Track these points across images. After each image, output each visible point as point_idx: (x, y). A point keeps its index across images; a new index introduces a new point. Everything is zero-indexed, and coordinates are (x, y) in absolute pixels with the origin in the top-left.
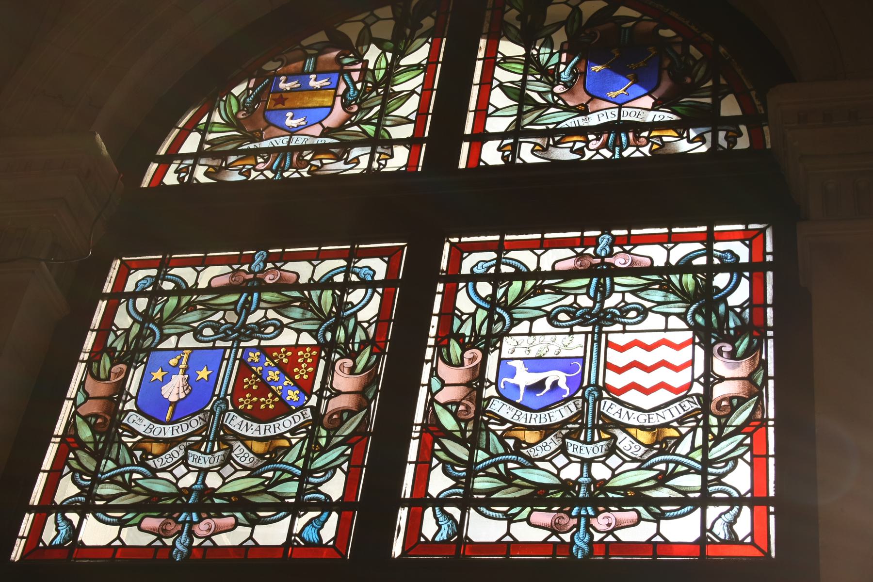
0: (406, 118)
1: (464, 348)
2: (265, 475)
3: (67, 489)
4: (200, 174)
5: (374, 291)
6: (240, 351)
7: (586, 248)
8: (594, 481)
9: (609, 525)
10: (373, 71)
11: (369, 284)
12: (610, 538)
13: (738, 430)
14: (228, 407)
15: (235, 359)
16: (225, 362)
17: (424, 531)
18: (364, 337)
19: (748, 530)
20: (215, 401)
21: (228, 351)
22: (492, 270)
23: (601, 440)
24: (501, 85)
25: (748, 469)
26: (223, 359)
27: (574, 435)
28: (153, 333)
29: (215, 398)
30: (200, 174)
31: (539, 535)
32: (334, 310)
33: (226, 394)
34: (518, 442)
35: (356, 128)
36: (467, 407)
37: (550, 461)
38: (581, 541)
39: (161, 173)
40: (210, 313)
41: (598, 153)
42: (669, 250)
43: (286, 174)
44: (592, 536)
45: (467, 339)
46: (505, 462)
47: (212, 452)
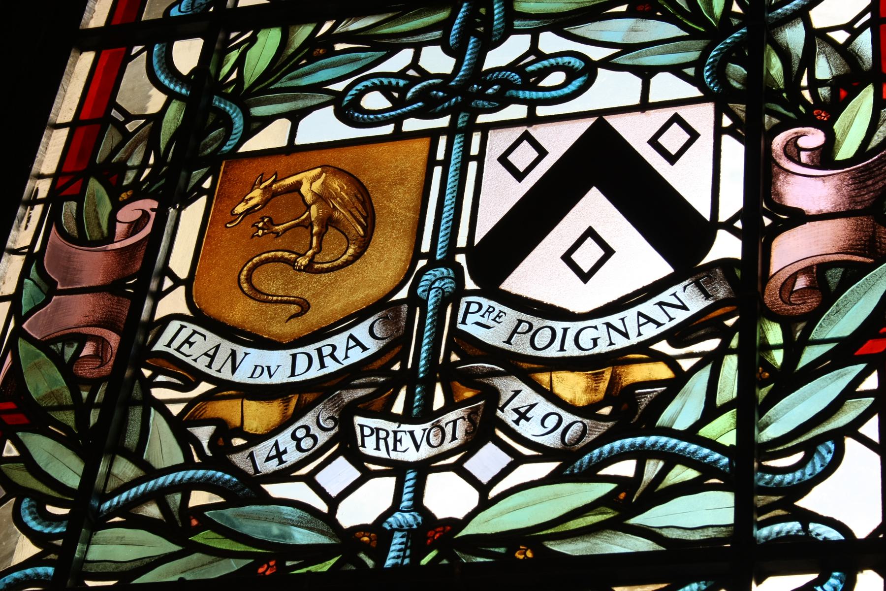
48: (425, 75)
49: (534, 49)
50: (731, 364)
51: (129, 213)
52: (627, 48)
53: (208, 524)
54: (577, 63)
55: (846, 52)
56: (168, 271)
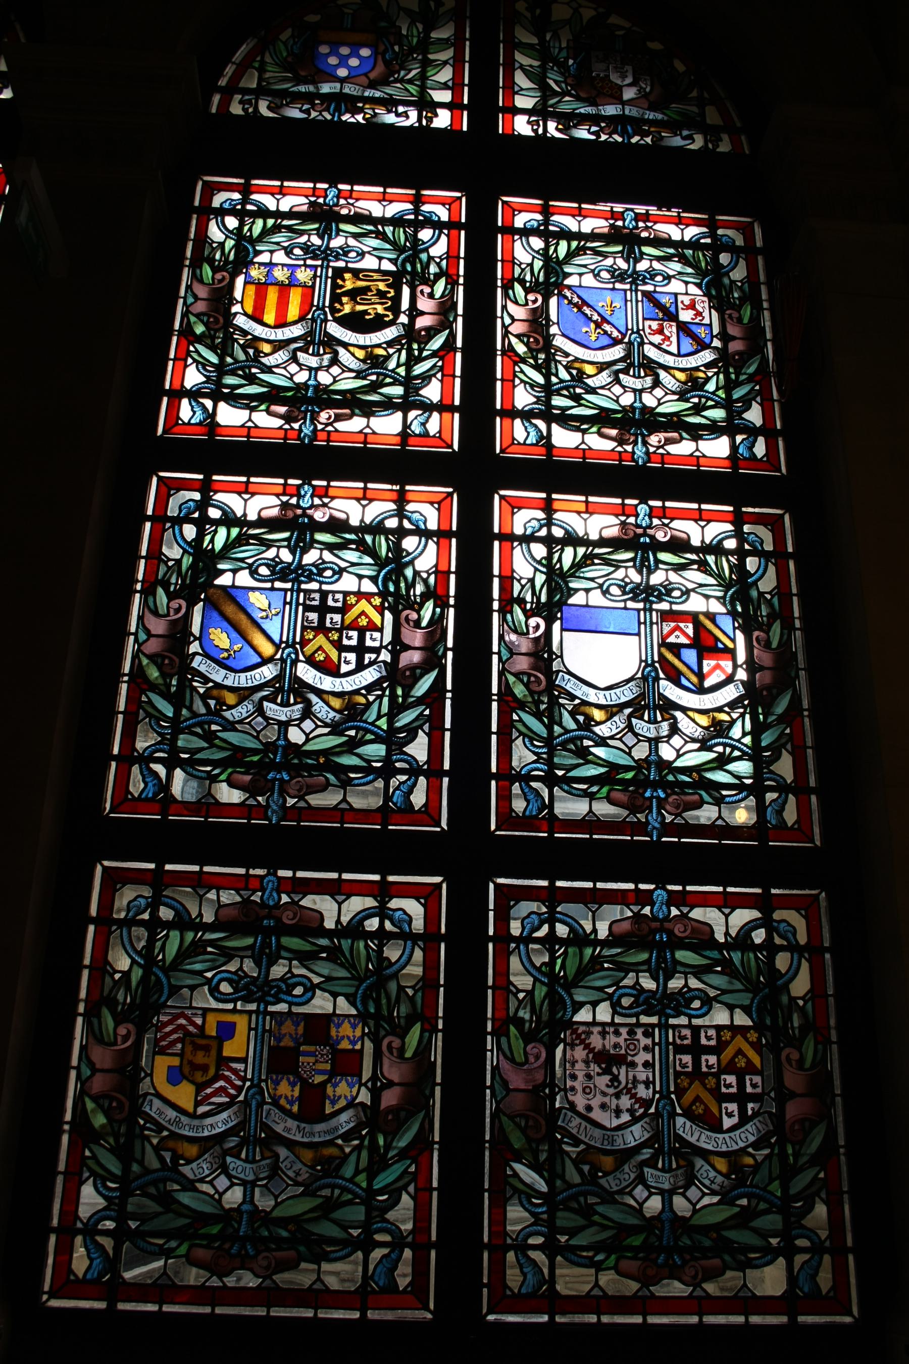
0: (445, 84)
1: (527, 291)
2: (369, 378)
4: (263, 109)
5: (441, 233)
6: (330, 270)
8: (644, 406)
9: (659, 442)
10: (407, 36)
11: (438, 226)
12: (661, 451)
15: (327, 277)
17: (515, 436)
18: (437, 270)
20: (315, 311)
23: (646, 375)
24: (522, 67)
27: (626, 371)
29: (314, 308)
30: (263, 109)
31: (609, 445)
32: (408, 244)
34: (581, 372)
35: (399, 85)
37: (609, 389)
38: (640, 451)
39: (225, 104)
41: (611, 137)
42: (682, 230)
43: (344, 118)
44: (648, 449)
45: (528, 284)
47: (318, 355)
48: (282, 562)
51: (174, 604)
52: (353, 564)
54: (336, 568)
55: (425, 581)
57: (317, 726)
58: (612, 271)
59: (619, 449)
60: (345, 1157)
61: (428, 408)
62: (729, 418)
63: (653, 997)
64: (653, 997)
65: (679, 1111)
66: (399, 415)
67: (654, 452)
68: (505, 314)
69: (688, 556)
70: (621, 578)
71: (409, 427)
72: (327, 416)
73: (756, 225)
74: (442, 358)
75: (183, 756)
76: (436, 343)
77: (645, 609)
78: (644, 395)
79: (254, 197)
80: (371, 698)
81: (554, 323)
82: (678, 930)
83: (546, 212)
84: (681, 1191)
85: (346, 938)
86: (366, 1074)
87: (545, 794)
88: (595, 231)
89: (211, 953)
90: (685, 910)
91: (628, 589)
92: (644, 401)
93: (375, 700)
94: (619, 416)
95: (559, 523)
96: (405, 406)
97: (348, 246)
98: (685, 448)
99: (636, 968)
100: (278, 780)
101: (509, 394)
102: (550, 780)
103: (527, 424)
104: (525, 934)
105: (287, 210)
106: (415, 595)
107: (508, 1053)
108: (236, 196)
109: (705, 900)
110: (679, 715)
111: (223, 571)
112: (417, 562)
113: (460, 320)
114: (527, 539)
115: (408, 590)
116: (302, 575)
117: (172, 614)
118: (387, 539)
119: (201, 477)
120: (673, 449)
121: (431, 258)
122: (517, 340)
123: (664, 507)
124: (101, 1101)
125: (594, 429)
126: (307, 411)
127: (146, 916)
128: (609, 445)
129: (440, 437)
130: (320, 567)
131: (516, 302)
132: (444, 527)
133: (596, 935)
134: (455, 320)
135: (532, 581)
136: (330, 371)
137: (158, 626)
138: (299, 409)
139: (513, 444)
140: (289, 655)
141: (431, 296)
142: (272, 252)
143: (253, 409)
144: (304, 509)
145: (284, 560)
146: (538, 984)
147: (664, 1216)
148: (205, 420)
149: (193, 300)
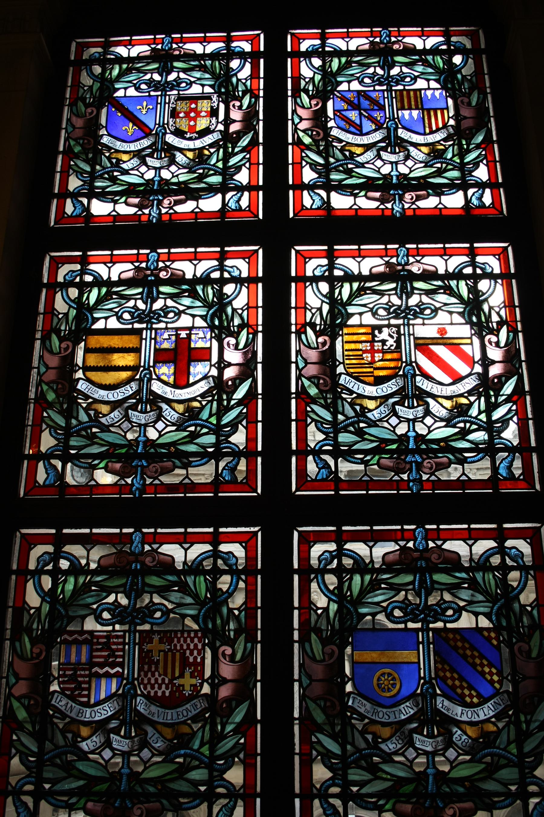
3: (74, 183)
7: (375, 38)
9: (412, 199)
13: (478, 147)
14: (166, 130)
16: (159, 106)
17: (305, 203)
18: (244, 88)
19: (491, 201)
21: (160, 98)
22: (320, 50)
25: (486, 168)
26: (157, 103)
28: (108, 87)
31: (374, 205)
33: (164, 124)
36: (317, 132)
37: (373, 164)
40: (142, 75)
42: (424, 40)
44: (403, 205)
46: (347, 164)
49: (165, 305)
50: (215, 403)
51: (64, 345)
52: (189, 308)
53: (97, 437)
55: (241, 316)
56: (77, 365)
57: (167, 426)
58: (372, 77)
59: (382, 207)
60: (194, 734)
61: (240, 189)
62: (463, 177)
63: (417, 609)
64: (417, 609)
65: (438, 692)
66: (219, 196)
67: (409, 208)
68: (295, 117)
69: (435, 283)
70: (385, 302)
71: (227, 205)
72: (168, 202)
73: (480, 31)
74: (249, 152)
75: (72, 452)
76: (245, 142)
77: (404, 324)
78: (399, 166)
79: (112, 49)
80: (204, 403)
81: (331, 119)
82: (434, 557)
83: (323, 38)
84: (441, 752)
85: (190, 575)
86: (208, 673)
87: (332, 463)
88: (360, 48)
89: (94, 590)
90: (439, 543)
91: (391, 310)
92: (399, 170)
93: (206, 404)
94: (381, 182)
95: (340, 266)
96: (223, 189)
97: (180, 79)
98: (431, 202)
99: (115, 590)
100: (140, 466)
101: (298, 174)
102: (336, 453)
103: (312, 194)
104: (321, 566)
105: (136, 55)
106: (233, 326)
107: (310, 654)
108: (100, 50)
109: (454, 535)
110: (430, 400)
111: (98, 319)
112: (233, 302)
113: (261, 123)
114: (315, 279)
115: (229, 324)
116: (153, 318)
117: (62, 351)
118: (213, 288)
119: (80, 253)
120: (422, 204)
121: (238, 80)
122: (303, 134)
123: (417, 248)
124: (23, 700)
125: (363, 193)
126: (154, 200)
127: (50, 567)
128: (374, 205)
129: (249, 210)
130: (165, 310)
131: (303, 107)
132: (253, 275)
133: (373, 565)
134: (258, 123)
135: (320, 309)
136: (170, 169)
137: (53, 362)
138: (148, 199)
139: (302, 209)
140: (145, 376)
141: (240, 108)
142: (126, 89)
143: (115, 202)
144: (152, 271)
145: (140, 308)
146: (331, 603)
147: (429, 771)
148: (83, 212)
149: (72, 129)
